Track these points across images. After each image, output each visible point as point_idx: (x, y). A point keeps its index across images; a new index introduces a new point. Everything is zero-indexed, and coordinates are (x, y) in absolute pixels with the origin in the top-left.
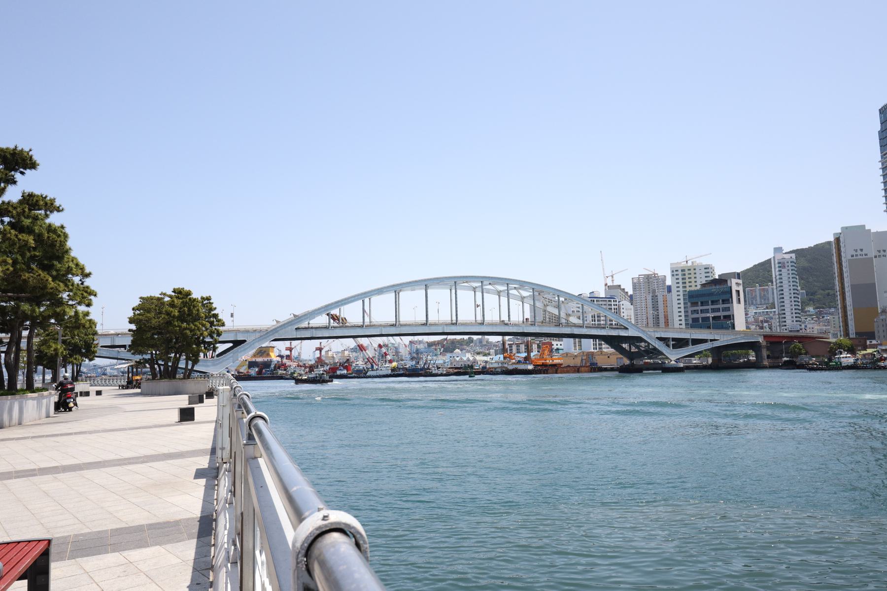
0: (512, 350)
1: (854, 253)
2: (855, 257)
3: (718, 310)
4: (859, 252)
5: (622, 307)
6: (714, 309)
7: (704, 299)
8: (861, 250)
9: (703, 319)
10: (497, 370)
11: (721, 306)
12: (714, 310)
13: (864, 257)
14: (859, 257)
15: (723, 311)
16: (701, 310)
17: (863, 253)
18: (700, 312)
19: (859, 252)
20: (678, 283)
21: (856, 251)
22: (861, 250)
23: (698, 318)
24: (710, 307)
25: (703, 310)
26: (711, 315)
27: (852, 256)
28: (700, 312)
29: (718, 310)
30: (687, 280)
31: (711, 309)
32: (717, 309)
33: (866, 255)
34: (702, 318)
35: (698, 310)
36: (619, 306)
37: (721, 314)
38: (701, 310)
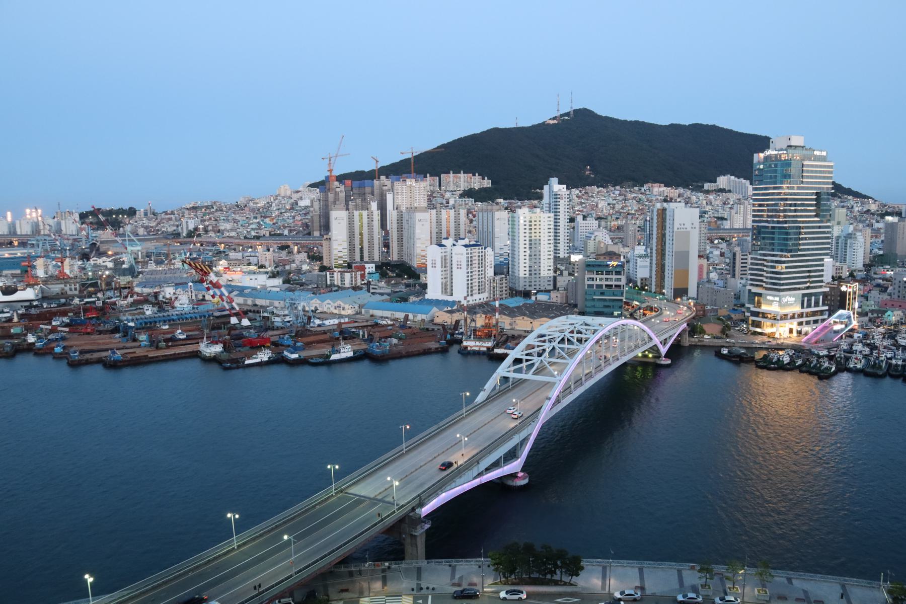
0: (333, 277)
1: (679, 227)
2: (679, 230)
3: (611, 280)
4: (682, 226)
5: (487, 253)
8: (684, 224)
11: (614, 277)
12: (607, 280)
13: (685, 230)
14: (682, 230)
15: (615, 281)
17: (685, 227)
19: (682, 226)
20: (525, 229)
21: (680, 225)
22: (684, 224)
23: (593, 285)
27: (678, 229)
29: (611, 280)
30: (533, 227)
33: (686, 228)
36: (485, 254)
37: (613, 283)
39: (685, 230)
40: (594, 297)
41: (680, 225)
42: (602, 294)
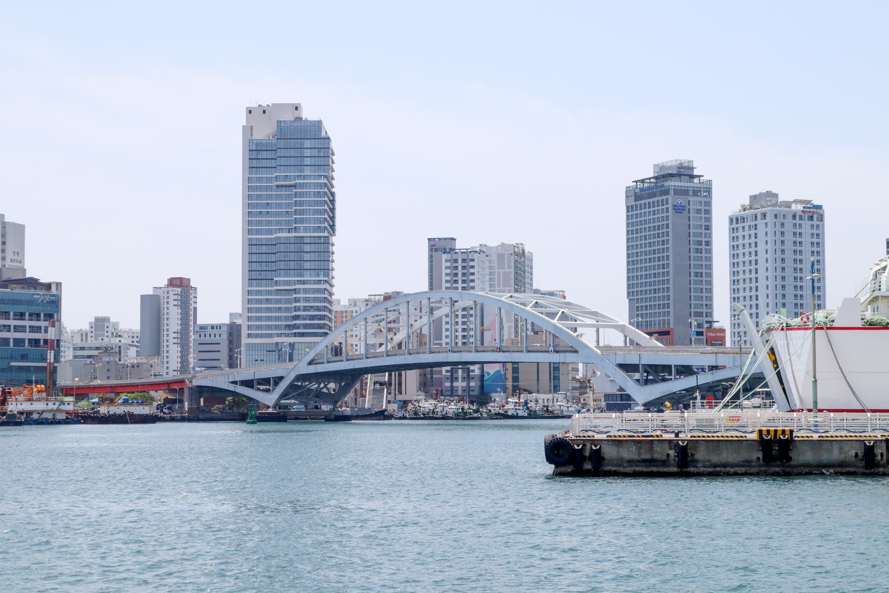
6: (32, 327)
7: (20, 309)
9: (19, 342)
10: (45, 415)
16: (15, 326)
18: (12, 329)
23: (8, 339)
24: (27, 323)
25: (18, 326)
26: (27, 336)
28: (12, 329)
31: (30, 327)
32: (38, 327)
34: (15, 339)
35: (9, 326)
38: (15, 326)
39: (18, 264)
40: (13, 364)
41: (14, 252)
42: (24, 357)
